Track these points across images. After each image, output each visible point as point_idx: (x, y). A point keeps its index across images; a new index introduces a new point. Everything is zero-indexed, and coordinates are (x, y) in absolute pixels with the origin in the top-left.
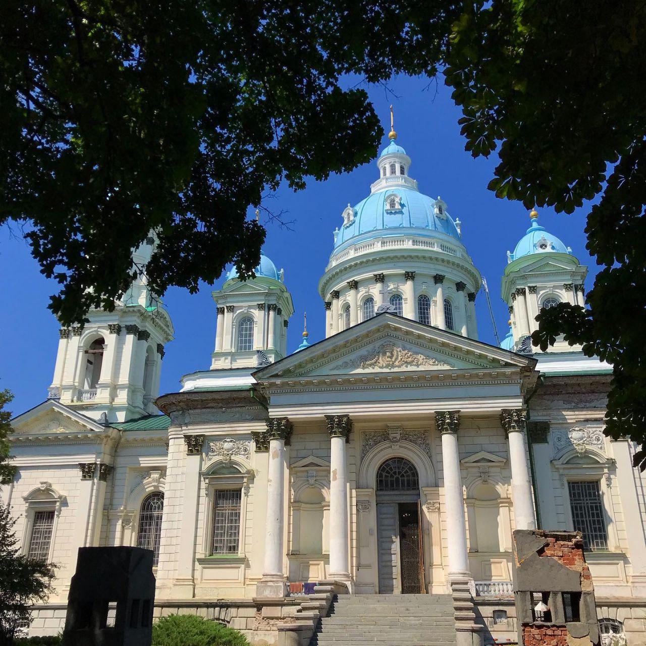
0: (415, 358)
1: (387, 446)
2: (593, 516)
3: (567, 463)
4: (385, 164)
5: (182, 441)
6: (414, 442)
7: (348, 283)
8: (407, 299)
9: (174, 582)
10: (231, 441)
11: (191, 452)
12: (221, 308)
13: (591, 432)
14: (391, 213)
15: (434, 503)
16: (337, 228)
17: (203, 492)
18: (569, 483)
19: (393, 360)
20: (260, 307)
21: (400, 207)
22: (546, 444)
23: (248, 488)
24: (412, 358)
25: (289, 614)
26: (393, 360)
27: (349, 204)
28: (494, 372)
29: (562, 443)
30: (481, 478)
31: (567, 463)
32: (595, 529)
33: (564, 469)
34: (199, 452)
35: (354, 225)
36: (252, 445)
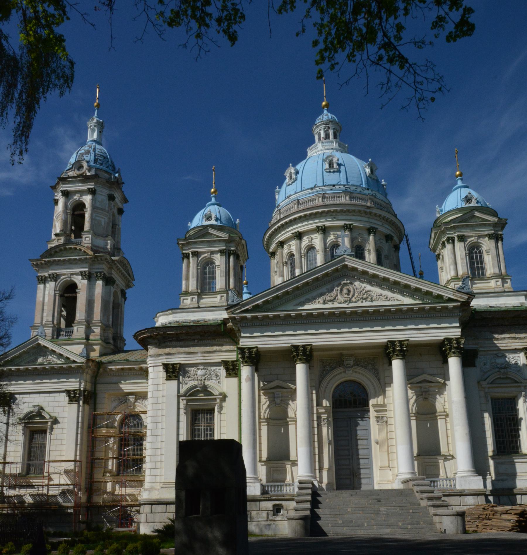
0: (369, 295)
2: (511, 426)
3: (491, 383)
4: (320, 130)
5: (161, 368)
6: (365, 367)
7: (292, 234)
9: (161, 485)
10: (204, 369)
11: (169, 378)
12: (186, 254)
13: (511, 358)
14: (330, 172)
15: (382, 417)
16: (277, 187)
17: (182, 411)
18: (492, 399)
19: (350, 296)
20: (222, 252)
21: (337, 167)
22: (475, 368)
23: (221, 408)
24: (367, 295)
25: (266, 508)
26: (350, 296)
27: (291, 164)
29: (487, 367)
30: (422, 396)
31: (491, 383)
32: (512, 435)
33: (489, 388)
34: (177, 378)
35: (296, 182)
36: (222, 371)
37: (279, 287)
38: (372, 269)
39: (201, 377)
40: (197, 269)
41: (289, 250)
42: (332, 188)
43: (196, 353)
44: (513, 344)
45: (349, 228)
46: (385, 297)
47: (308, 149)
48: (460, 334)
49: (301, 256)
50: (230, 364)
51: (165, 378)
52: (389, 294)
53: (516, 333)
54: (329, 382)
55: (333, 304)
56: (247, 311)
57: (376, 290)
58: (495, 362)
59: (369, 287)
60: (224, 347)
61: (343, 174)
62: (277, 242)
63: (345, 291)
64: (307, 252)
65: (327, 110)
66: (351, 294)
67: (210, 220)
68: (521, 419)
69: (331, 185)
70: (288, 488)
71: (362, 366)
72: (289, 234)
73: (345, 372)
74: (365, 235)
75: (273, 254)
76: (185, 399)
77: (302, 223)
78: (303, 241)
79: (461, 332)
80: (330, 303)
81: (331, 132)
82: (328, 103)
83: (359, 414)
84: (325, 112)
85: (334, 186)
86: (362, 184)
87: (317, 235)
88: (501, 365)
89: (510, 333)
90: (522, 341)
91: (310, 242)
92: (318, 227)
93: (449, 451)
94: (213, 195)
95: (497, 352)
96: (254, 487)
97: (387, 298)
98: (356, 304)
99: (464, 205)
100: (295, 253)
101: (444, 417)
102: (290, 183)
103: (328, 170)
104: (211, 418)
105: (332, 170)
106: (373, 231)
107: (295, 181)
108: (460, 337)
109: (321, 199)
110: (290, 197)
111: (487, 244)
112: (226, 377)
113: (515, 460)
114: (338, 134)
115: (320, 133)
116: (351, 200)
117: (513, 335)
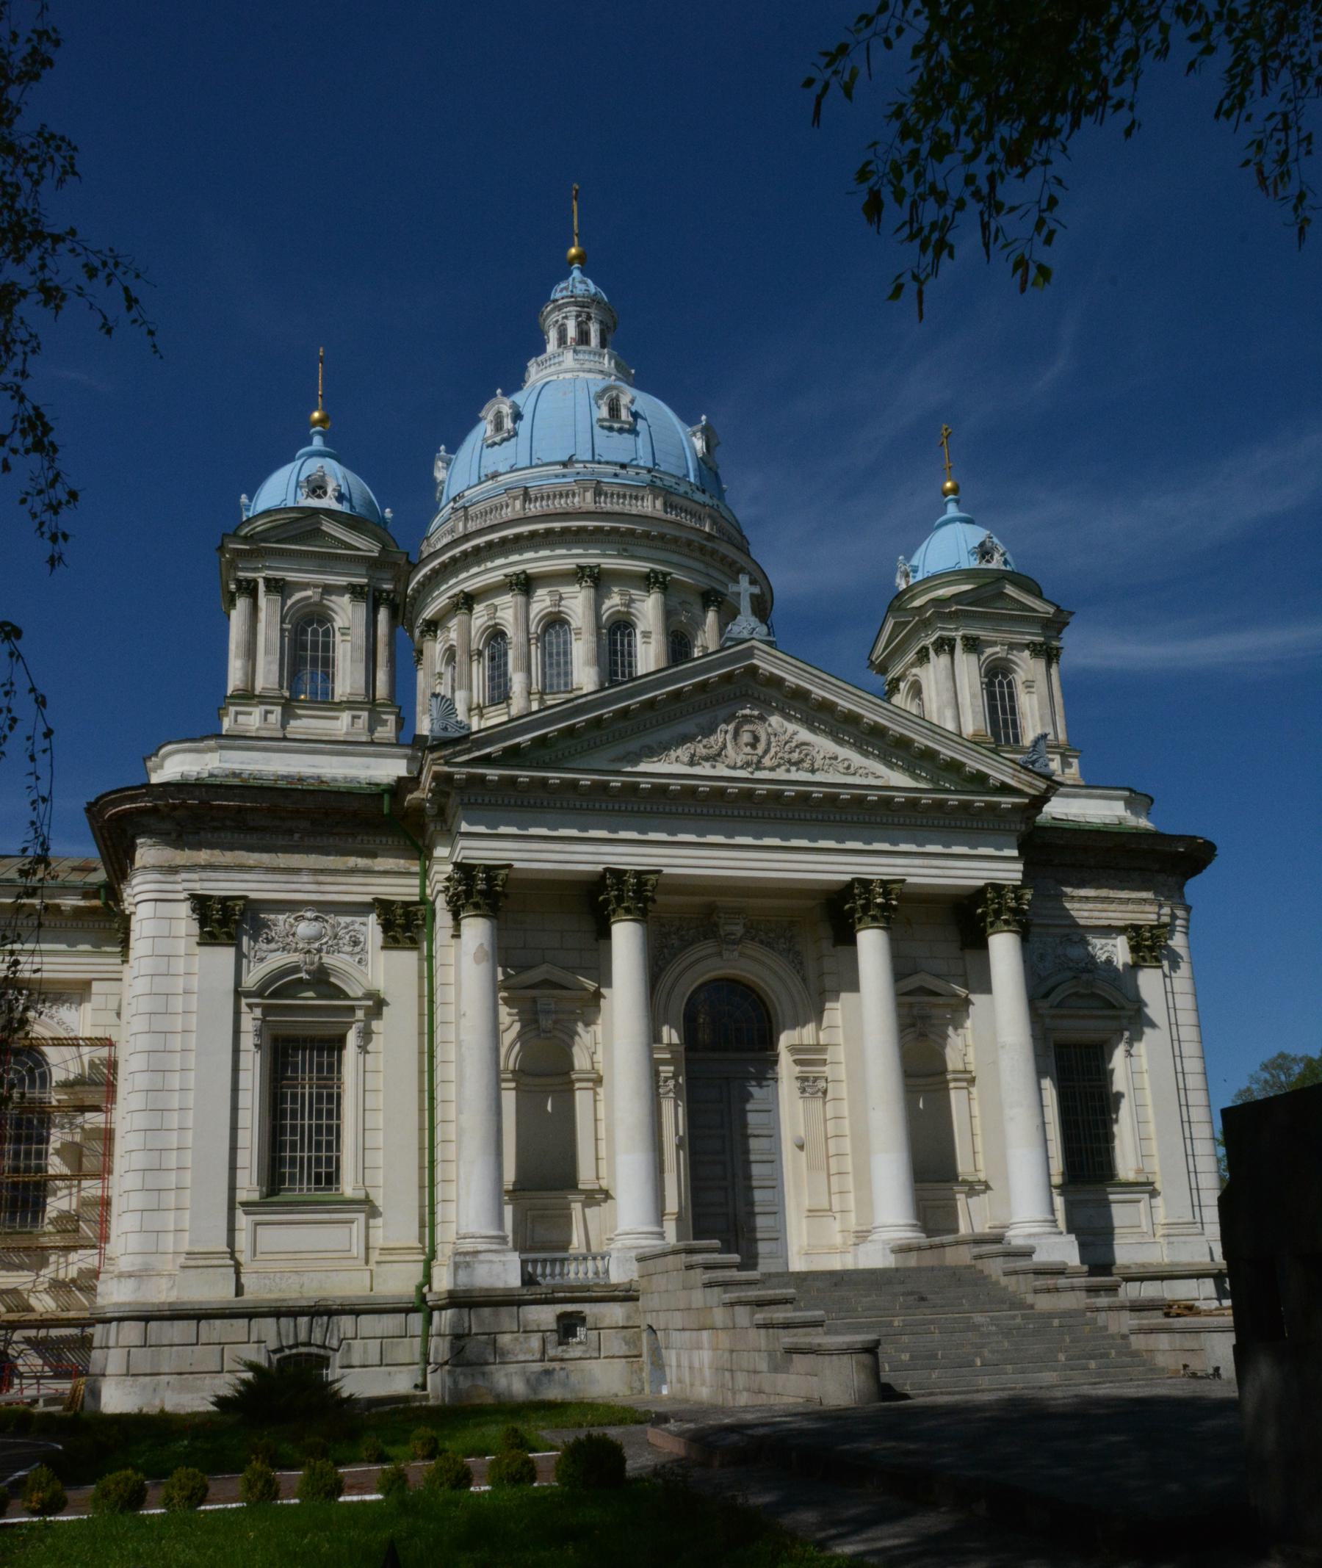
0: (807, 755)
1: (710, 951)
4: (566, 318)
5: (184, 909)
6: (769, 945)
7: (506, 576)
8: (650, 632)
10: (316, 919)
11: (209, 938)
12: (248, 581)
14: (611, 429)
15: (816, 1079)
17: (248, 1041)
19: (760, 751)
20: (356, 592)
21: (631, 419)
23: (366, 1035)
24: (800, 753)
25: (538, 1325)
26: (760, 751)
27: (499, 391)
28: (979, 800)
30: (913, 1029)
33: (1053, 1017)
34: (232, 940)
35: (513, 440)
36: (371, 928)
37: (579, 705)
38: (823, 688)
39: (309, 943)
40: (282, 630)
41: (490, 619)
42: (618, 470)
43: (297, 871)
44: (1104, 914)
45: (661, 583)
46: (845, 765)
47: (533, 360)
48: (1020, 876)
49: (529, 640)
50: (400, 911)
51: (197, 939)
52: (856, 759)
53: (1112, 888)
54: (677, 979)
55: (714, 767)
56: (487, 760)
57: (823, 745)
58: (1065, 955)
59: (804, 735)
60: (379, 860)
61: (642, 441)
62: (455, 595)
63: (746, 737)
64: (545, 630)
65: (582, 271)
66: (761, 747)
67: (319, 497)
68: (1119, 1096)
69: (616, 464)
70: (582, 1269)
71: (761, 942)
72: (496, 576)
73: (720, 954)
74: (697, 609)
75: (433, 626)
76: (257, 1005)
77: (536, 552)
78: (535, 599)
79: (1024, 873)
80: (707, 765)
81: (594, 329)
82: (584, 253)
83: (752, 1070)
84: (576, 274)
85: (623, 466)
86: (687, 475)
87: (577, 588)
88: (1077, 963)
89: (1098, 887)
90: (1123, 907)
91: (555, 605)
92: (581, 568)
93: (598, 1178)
94: (318, 428)
95: (1067, 931)
96: (504, 1263)
97: (848, 768)
98: (772, 773)
99: (974, 563)
100: (510, 632)
101: (964, 1084)
102: (497, 439)
103: (606, 424)
104: (330, 1066)
105: (616, 426)
106: (716, 600)
107: (513, 436)
108: (1019, 883)
109: (589, 495)
110: (500, 479)
111: (1027, 668)
112: (383, 948)
113: (1112, 1197)
114: (609, 337)
115: (563, 325)
116: (666, 512)
117: (1104, 893)
